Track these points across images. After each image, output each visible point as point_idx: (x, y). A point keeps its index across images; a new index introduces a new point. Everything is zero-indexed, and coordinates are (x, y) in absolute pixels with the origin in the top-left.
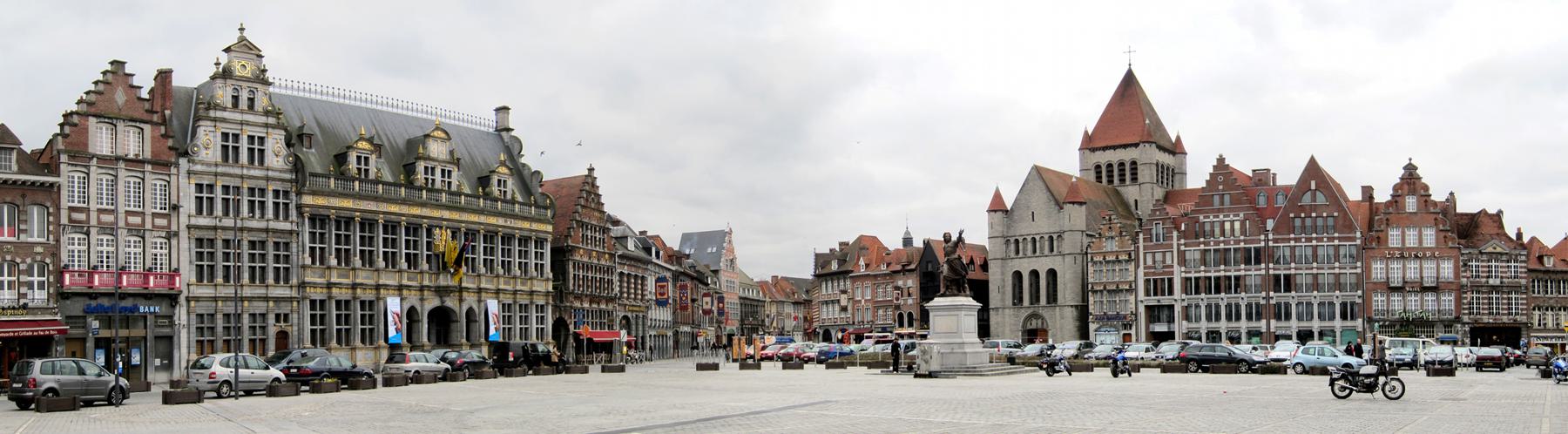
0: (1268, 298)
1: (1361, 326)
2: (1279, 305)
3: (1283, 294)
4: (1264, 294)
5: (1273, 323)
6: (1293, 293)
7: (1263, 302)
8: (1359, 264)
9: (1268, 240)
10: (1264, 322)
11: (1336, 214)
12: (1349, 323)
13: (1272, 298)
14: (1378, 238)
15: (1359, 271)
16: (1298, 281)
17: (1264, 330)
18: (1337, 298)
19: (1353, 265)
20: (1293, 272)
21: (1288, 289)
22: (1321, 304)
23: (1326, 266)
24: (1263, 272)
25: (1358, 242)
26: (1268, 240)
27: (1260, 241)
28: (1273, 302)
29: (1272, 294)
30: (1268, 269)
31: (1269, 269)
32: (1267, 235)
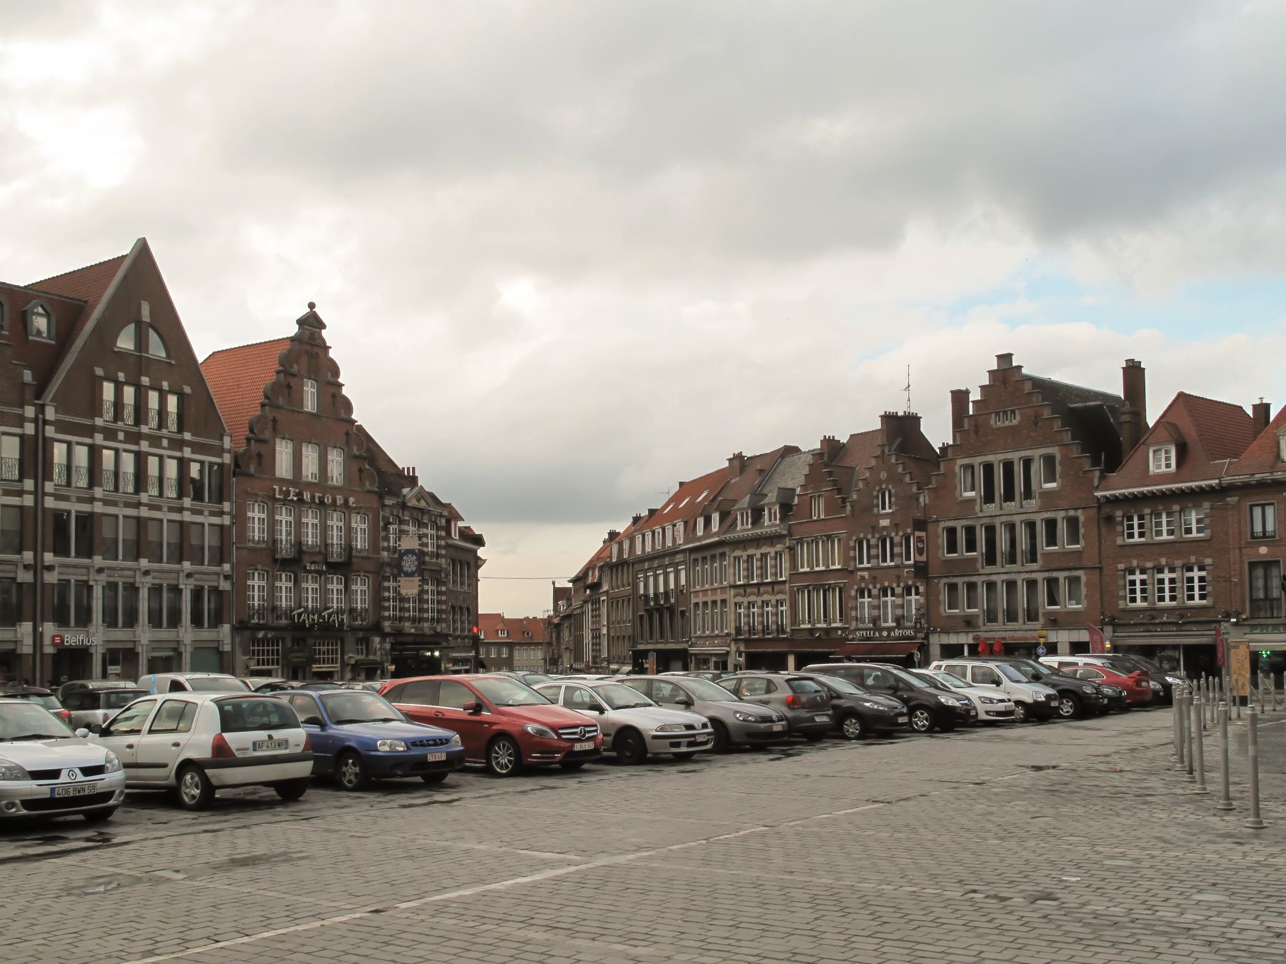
0: (37, 568)
1: (228, 640)
2: (64, 585)
3: (72, 560)
4: (28, 556)
5: (49, 629)
6: (98, 560)
7: (25, 577)
8: (226, 506)
9: (35, 421)
10: (27, 627)
11: (187, 390)
12: (206, 634)
13: (50, 568)
14: (259, 456)
15: (226, 520)
16: (107, 533)
17: (27, 648)
18: (188, 577)
19: (215, 507)
20: (98, 508)
21: (87, 550)
22: (156, 590)
23: (206, 505)
24: (28, 501)
25: (227, 459)
26: (35, 421)
27: (21, 420)
28: (51, 578)
29: (49, 557)
30: (38, 493)
31: (35, 493)
32: (41, 409)
